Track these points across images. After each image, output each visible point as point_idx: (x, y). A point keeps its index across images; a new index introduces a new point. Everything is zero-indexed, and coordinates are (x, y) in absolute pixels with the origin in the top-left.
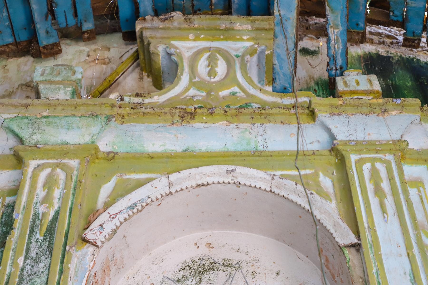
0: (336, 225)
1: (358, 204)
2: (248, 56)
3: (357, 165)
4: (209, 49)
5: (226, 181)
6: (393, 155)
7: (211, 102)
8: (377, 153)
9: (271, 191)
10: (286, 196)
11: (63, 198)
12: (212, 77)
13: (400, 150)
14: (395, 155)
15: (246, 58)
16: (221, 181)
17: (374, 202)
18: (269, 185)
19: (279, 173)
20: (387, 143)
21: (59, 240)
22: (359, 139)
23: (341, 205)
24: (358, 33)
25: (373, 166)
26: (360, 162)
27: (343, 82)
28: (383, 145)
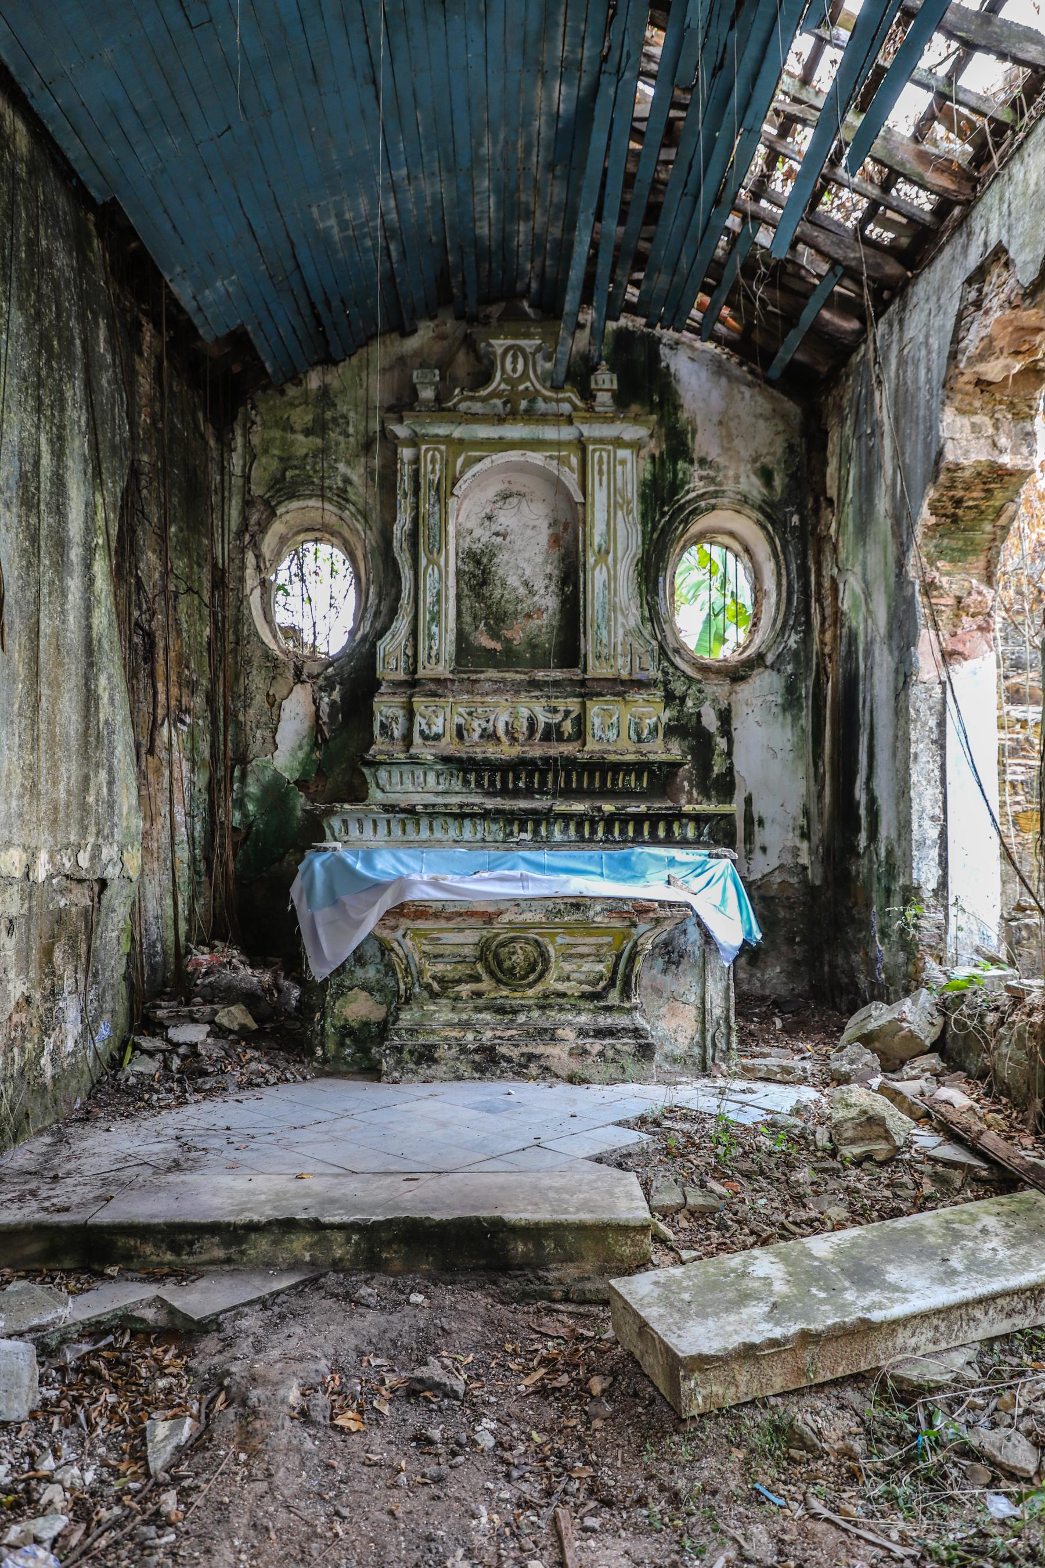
11: (441, 470)
21: (443, 495)
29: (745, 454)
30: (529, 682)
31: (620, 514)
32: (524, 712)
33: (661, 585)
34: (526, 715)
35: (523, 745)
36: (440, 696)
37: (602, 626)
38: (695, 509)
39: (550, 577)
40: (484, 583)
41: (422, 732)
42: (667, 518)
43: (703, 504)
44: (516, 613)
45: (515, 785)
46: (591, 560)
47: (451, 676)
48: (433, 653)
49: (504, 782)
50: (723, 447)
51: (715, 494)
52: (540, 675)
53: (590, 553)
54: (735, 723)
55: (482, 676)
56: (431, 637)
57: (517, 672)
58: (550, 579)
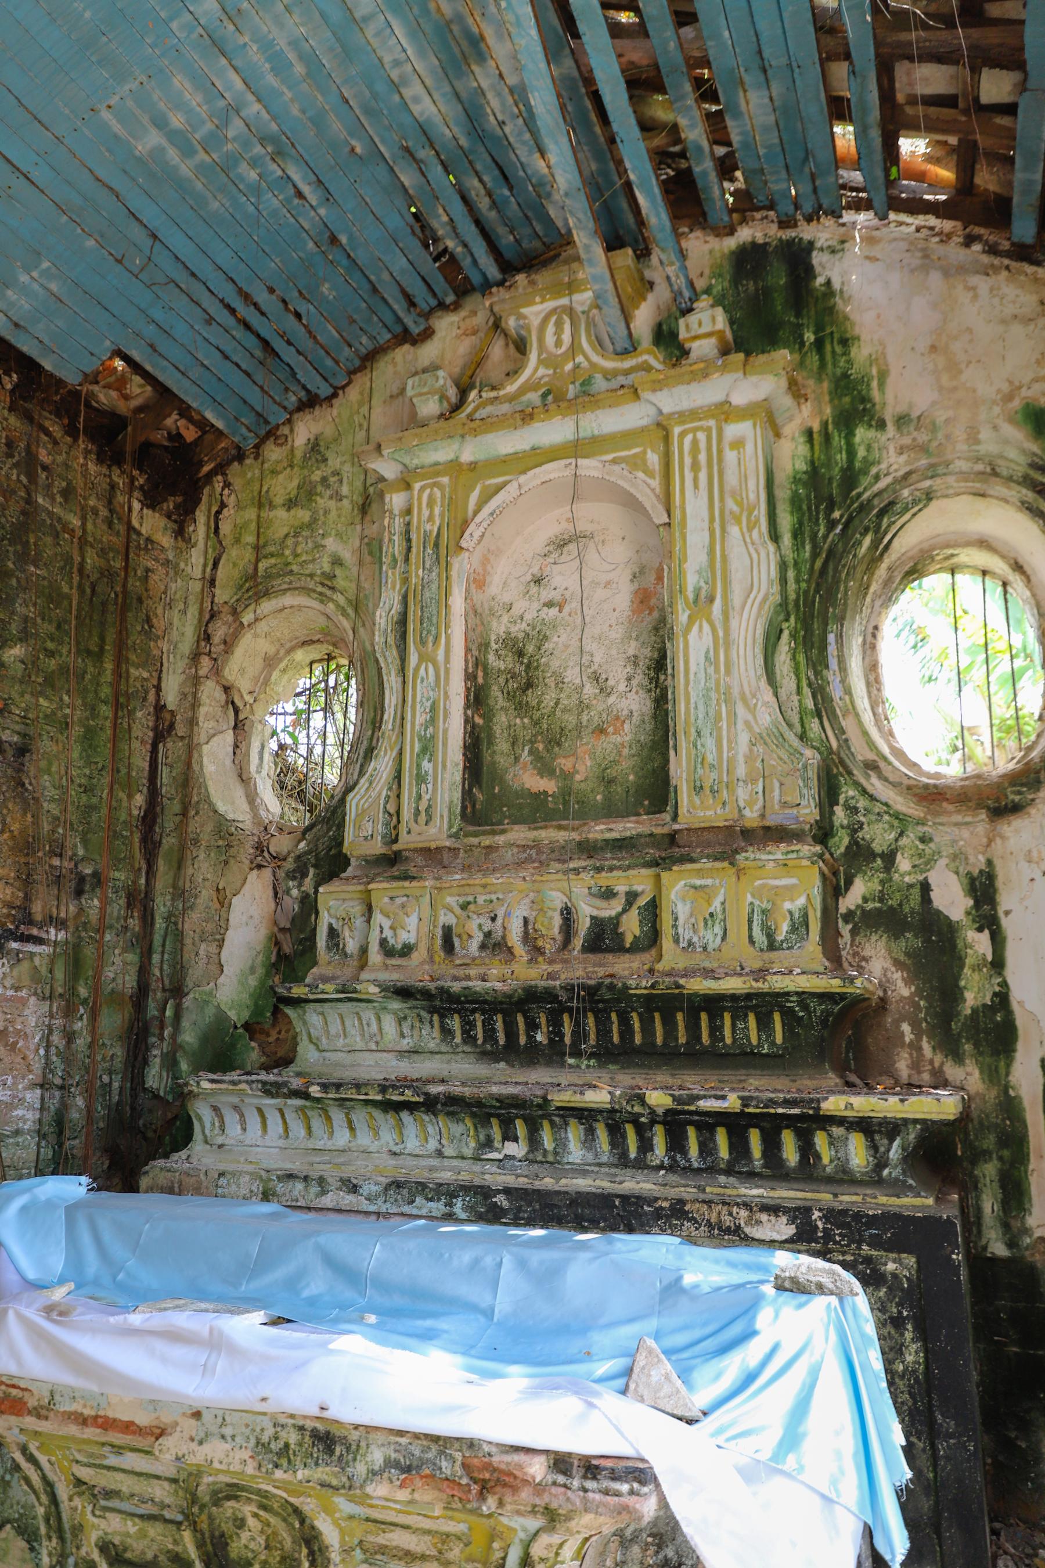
29: (987, 390)
30: (580, 844)
31: (734, 531)
32: (556, 899)
33: (832, 649)
34: (559, 905)
35: (551, 962)
36: (414, 878)
37: (706, 732)
38: (892, 504)
39: (635, 661)
40: (529, 685)
41: (383, 942)
42: (838, 530)
43: (906, 493)
44: (579, 727)
45: (531, 1038)
46: (683, 617)
47: (448, 844)
48: (422, 808)
49: (511, 1033)
50: (941, 389)
51: (932, 472)
52: (599, 831)
53: (680, 606)
54: (1006, 900)
55: (500, 839)
56: (420, 778)
57: (560, 828)
58: (635, 664)
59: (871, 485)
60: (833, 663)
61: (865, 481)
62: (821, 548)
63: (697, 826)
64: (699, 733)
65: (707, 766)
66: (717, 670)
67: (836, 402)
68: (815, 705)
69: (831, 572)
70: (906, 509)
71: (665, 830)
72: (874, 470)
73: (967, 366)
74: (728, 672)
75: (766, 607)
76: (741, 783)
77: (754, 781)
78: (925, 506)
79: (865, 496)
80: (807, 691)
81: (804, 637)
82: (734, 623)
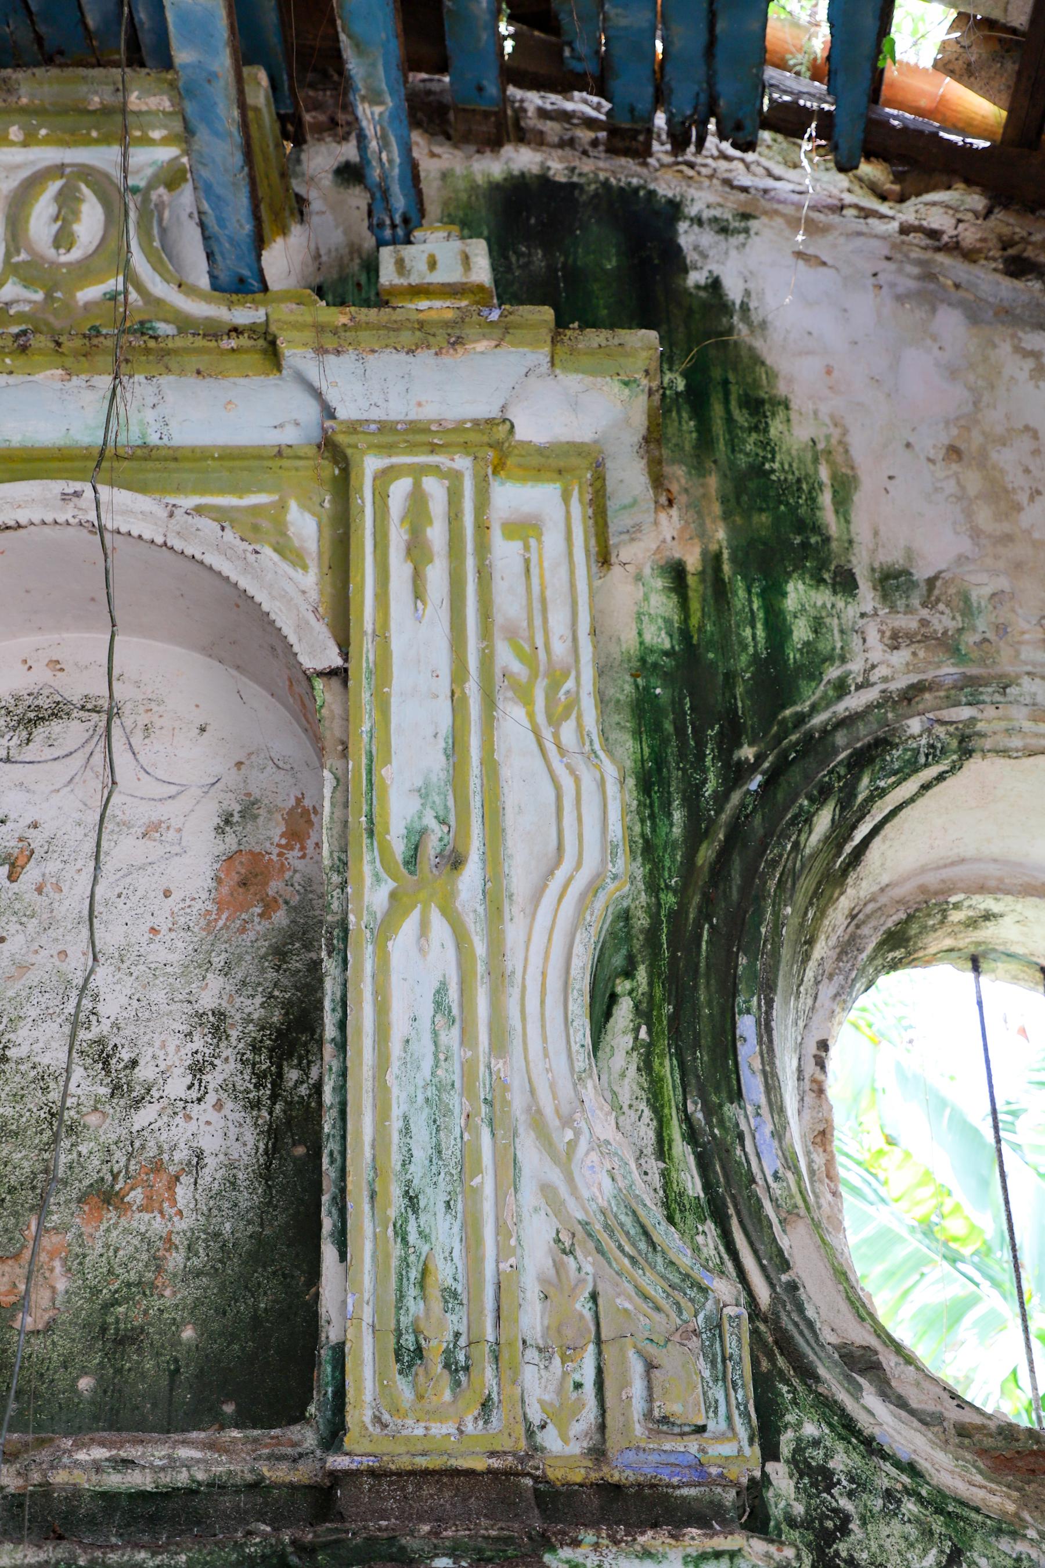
0: (301, 626)
1: (358, 578)
2: (162, 190)
3: (378, 482)
4: (58, 170)
5: (61, 519)
6: (471, 458)
7: (52, 319)
8: (432, 452)
9: (165, 544)
10: (198, 556)
12: (62, 251)
13: (491, 446)
14: (476, 458)
15: (154, 196)
16: (49, 519)
17: (400, 571)
18: (162, 530)
19: (190, 501)
20: (459, 428)
22: (394, 416)
23: (328, 579)
24: (486, 115)
25: (417, 486)
26: (385, 476)
27: (396, 263)
28: (447, 431)
37: (433, 1198)
38: (882, 744)
42: (755, 783)
43: (915, 725)
50: (976, 534)
59: (827, 702)
60: (753, 1086)
61: (811, 694)
62: (712, 822)
63: (404, 1463)
64: (412, 1201)
65: (434, 1293)
66: (467, 1037)
67: (738, 520)
68: (707, 1186)
69: (737, 879)
70: (912, 767)
71: (302, 1474)
72: (833, 673)
73: (1032, 499)
74: (499, 1043)
75: (599, 904)
76: (532, 1354)
77: (570, 1352)
78: (954, 769)
79: (818, 720)
80: (682, 1151)
81: (673, 1018)
82: (514, 932)
